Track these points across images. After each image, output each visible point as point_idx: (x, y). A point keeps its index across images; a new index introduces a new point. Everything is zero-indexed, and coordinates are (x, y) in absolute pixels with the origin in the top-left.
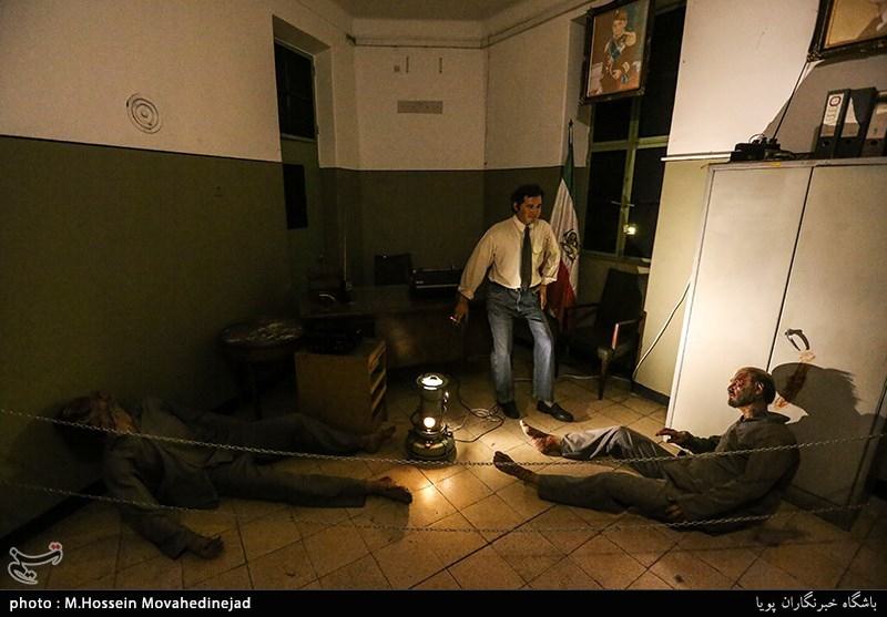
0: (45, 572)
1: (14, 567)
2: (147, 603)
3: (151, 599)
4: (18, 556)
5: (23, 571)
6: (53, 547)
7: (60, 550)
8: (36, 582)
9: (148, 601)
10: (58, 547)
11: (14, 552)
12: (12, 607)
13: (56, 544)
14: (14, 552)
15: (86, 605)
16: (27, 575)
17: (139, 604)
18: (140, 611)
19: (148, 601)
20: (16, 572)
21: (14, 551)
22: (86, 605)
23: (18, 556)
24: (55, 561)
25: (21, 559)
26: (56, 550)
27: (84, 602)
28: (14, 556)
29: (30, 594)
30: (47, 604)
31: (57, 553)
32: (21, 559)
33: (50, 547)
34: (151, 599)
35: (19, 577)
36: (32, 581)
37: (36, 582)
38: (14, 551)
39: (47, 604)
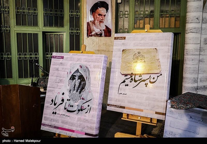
0: (10, 134)
1: (3, 132)
2: (27, 141)
3: (28, 140)
4: (4, 130)
5: (5, 133)
6: (12, 128)
7: (14, 128)
8: (8, 136)
9: (27, 140)
10: (13, 128)
11: (3, 129)
12: (3, 142)
13: (13, 127)
14: (3, 129)
15: (15, 141)
16: (6, 134)
17: (25, 141)
18: (25, 142)
19: (27, 140)
20: (3, 133)
21: (3, 129)
22: (15, 141)
23: (4, 130)
24: (13, 131)
25: (5, 130)
26: (13, 128)
27: (14, 141)
28: (3, 130)
29: (6, 138)
30: (10, 141)
31: (13, 129)
32: (5, 130)
33: (11, 128)
34: (28, 140)
35: (4, 135)
36: (7, 136)
37: (8, 136)
38: (3, 129)
39: (10, 141)
